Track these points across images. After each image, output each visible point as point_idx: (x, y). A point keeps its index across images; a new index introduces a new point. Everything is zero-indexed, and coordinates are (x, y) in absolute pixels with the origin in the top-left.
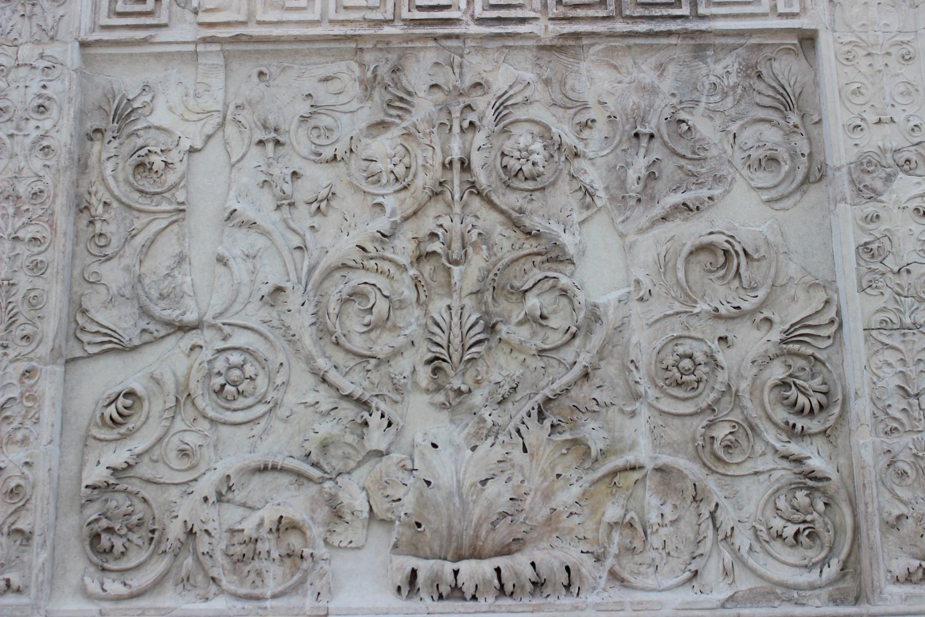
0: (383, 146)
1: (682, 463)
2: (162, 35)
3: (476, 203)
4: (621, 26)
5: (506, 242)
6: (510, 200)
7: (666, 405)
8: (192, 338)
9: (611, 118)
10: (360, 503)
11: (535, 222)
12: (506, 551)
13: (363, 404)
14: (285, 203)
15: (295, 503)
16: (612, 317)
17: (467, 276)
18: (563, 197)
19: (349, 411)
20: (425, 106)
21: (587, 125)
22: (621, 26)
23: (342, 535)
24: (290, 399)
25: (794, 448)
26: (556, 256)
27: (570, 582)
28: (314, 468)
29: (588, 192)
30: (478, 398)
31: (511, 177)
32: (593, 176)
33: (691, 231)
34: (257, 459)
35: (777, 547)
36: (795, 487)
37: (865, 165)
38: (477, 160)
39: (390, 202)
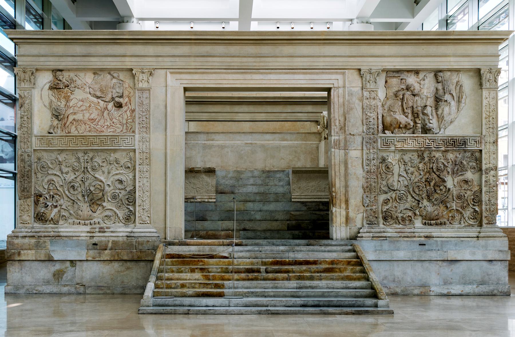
0: (421, 166)
1: (459, 209)
2: (390, 149)
3: (433, 174)
4: (455, 149)
5: (437, 179)
6: (438, 173)
7: (458, 201)
8: (396, 192)
9: (452, 162)
10: (418, 213)
11: (441, 176)
12: (437, 220)
13: (419, 201)
14: (407, 173)
15: (410, 214)
16: (451, 190)
17: (432, 184)
18: (445, 173)
19: (416, 202)
20: (426, 159)
21: (449, 162)
22: (455, 149)
23: (416, 217)
24: (409, 200)
25: (474, 207)
26: (444, 181)
27: (445, 224)
28: (411, 209)
29: (448, 172)
30: (433, 200)
31: (438, 170)
32: (449, 170)
33: (461, 178)
34: (405, 208)
35: (471, 220)
36: (473, 212)
37: (486, 169)
38: (434, 168)
39: (422, 173)
